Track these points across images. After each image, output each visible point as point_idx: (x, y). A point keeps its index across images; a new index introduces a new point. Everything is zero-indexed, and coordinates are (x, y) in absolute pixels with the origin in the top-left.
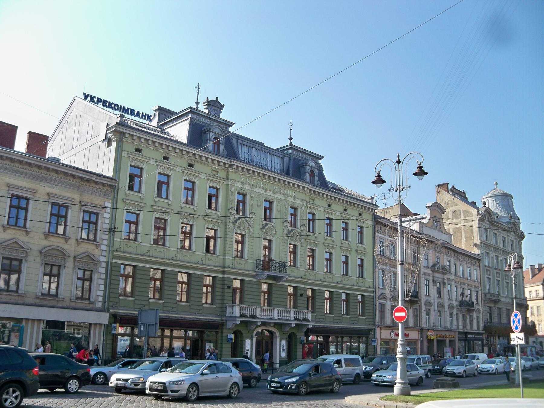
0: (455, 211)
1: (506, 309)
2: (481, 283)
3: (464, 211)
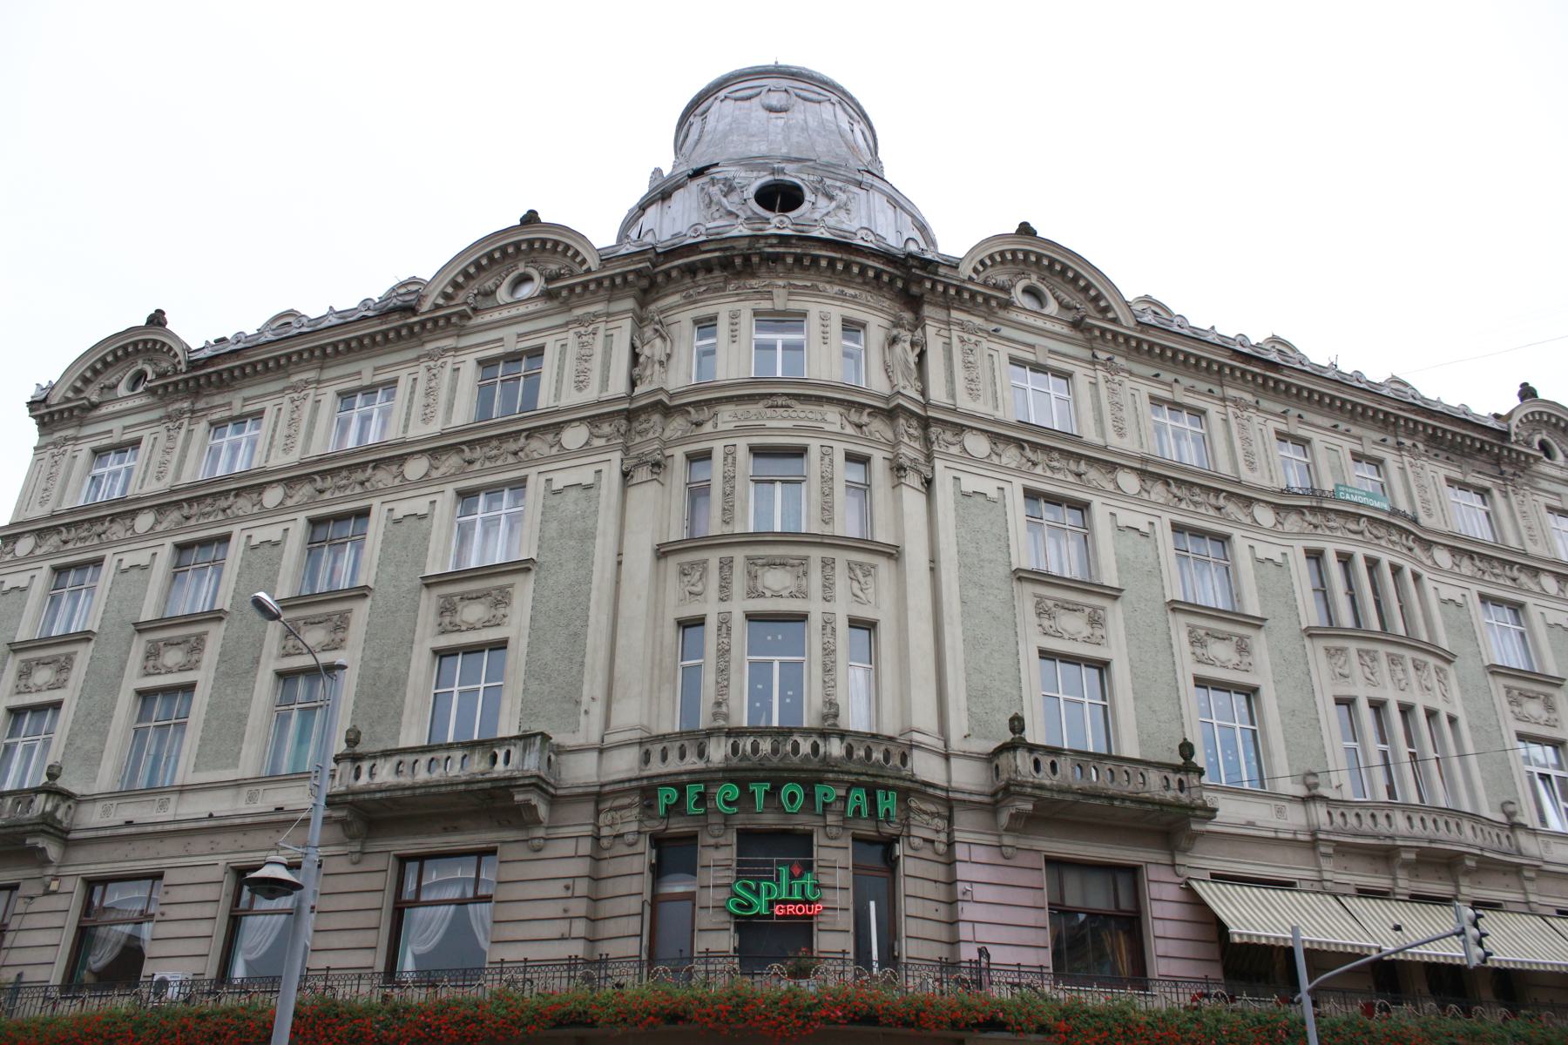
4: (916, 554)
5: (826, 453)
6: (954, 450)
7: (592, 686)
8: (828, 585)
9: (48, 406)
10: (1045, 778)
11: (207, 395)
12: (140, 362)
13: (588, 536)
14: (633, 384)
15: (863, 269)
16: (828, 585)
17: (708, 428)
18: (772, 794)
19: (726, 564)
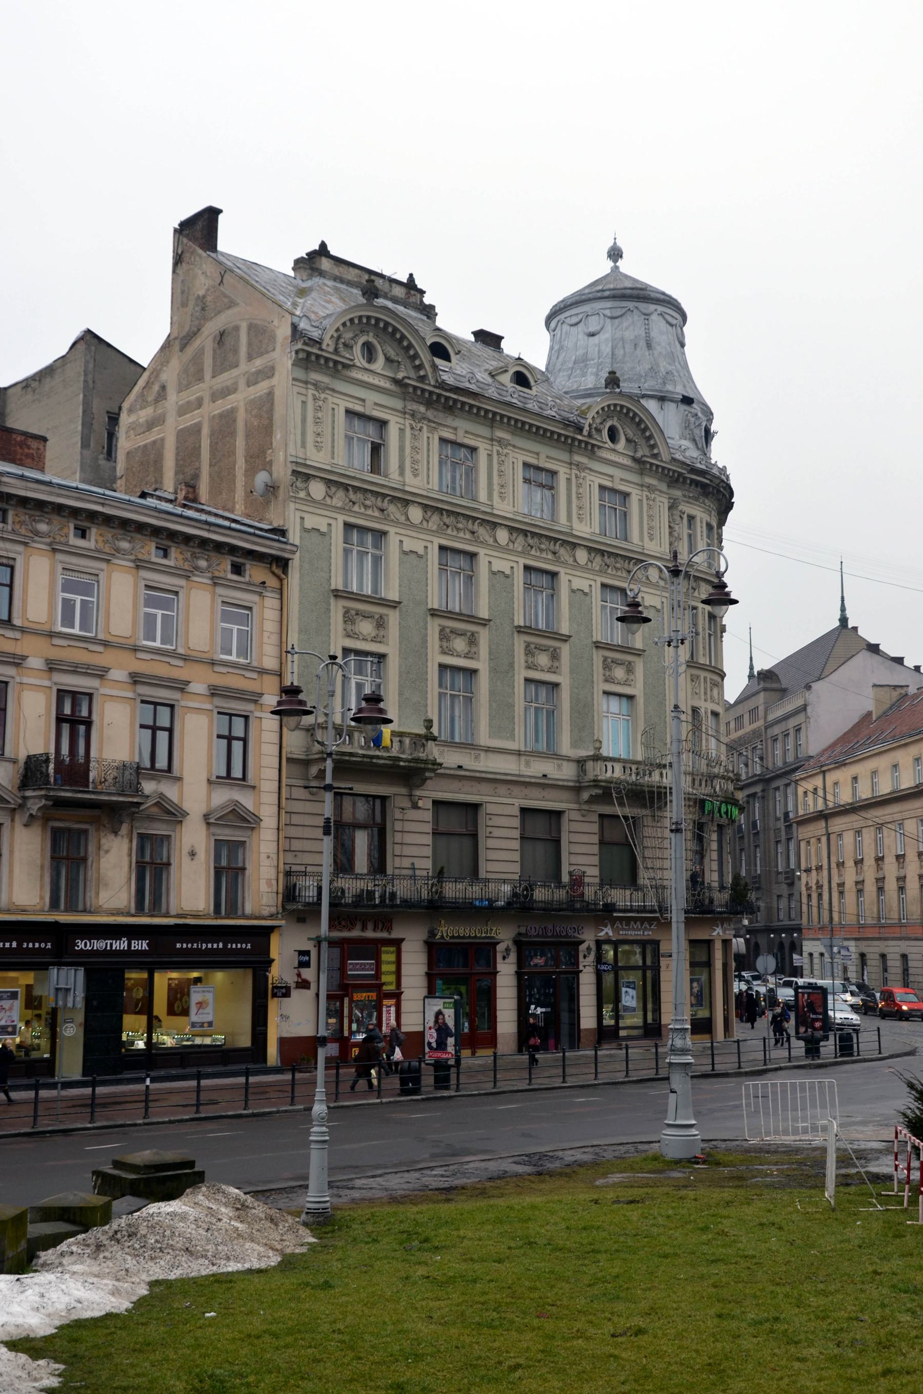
0: (222, 334)
1: (524, 811)
2: (280, 675)
3: (251, 327)
9: (321, 349)
11: (435, 409)
12: (371, 334)
17: (696, 594)
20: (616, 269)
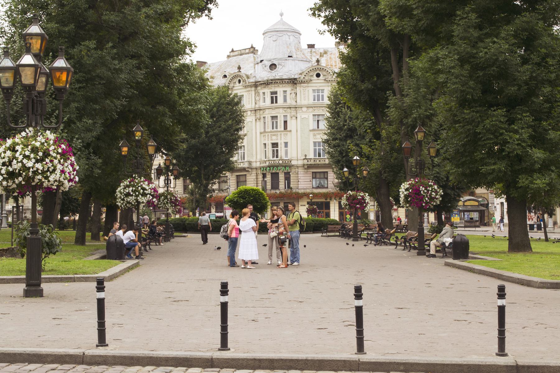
4: (294, 131)
5: (280, 116)
6: (301, 111)
7: (254, 153)
8: (281, 138)
10: (309, 163)
13: (252, 130)
14: (256, 103)
15: (285, 82)
16: (281, 138)
17: (265, 113)
18: (273, 169)
19: (268, 135)
20: (282, 19)
